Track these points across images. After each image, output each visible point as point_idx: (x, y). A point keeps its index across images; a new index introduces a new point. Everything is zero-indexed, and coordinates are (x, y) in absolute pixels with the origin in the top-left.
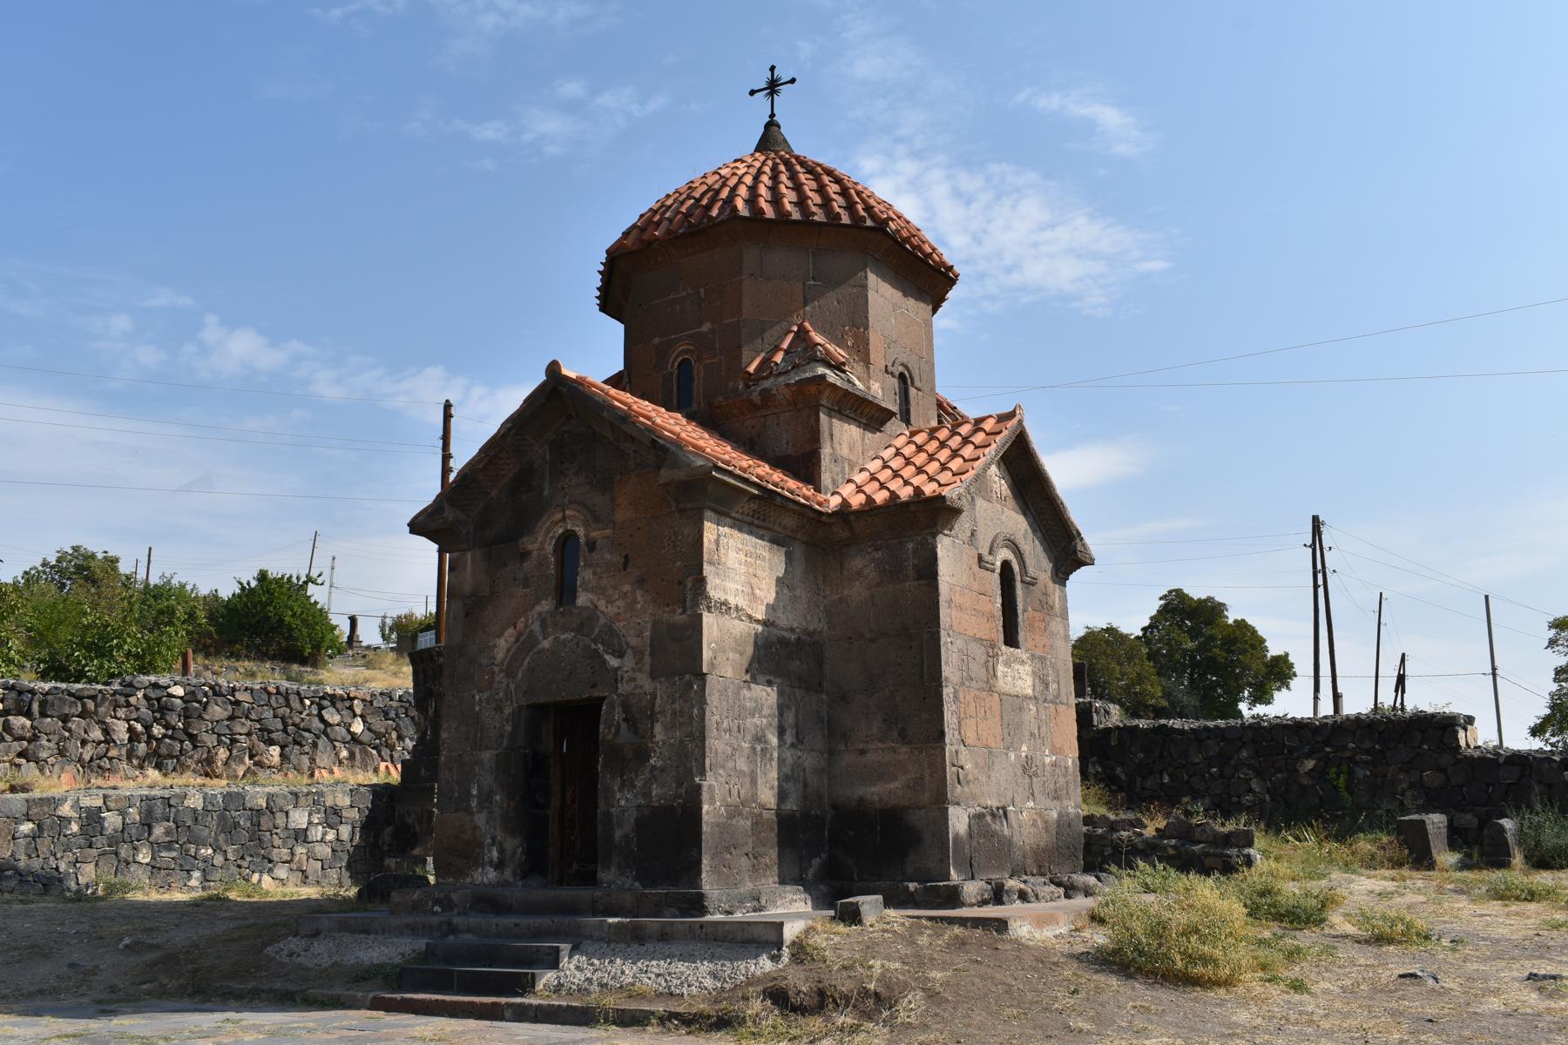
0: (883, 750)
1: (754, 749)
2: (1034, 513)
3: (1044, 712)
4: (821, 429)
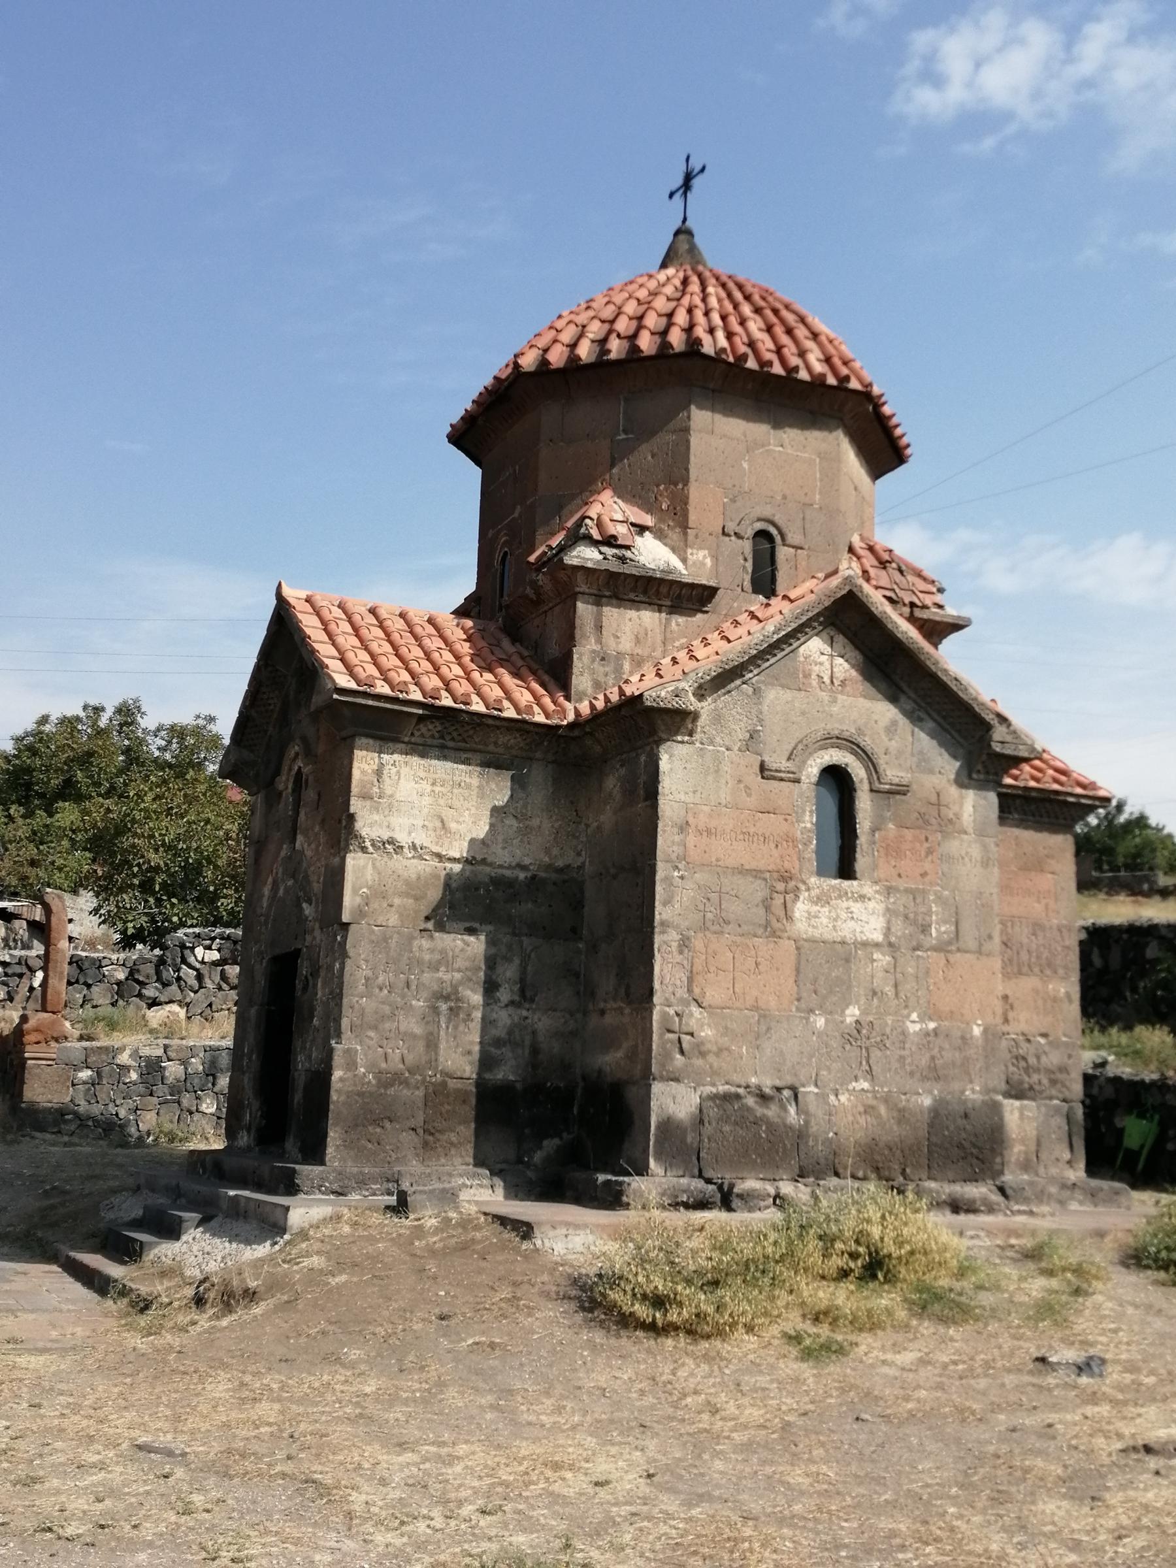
0: (615, 1009)
1: (435, 1010)
2: (913, 695)
3: (913, 963)
4: (578, 622)
